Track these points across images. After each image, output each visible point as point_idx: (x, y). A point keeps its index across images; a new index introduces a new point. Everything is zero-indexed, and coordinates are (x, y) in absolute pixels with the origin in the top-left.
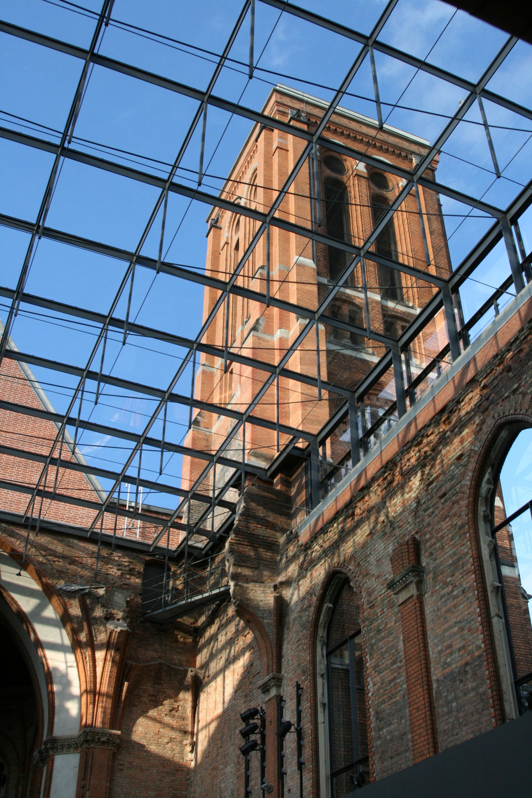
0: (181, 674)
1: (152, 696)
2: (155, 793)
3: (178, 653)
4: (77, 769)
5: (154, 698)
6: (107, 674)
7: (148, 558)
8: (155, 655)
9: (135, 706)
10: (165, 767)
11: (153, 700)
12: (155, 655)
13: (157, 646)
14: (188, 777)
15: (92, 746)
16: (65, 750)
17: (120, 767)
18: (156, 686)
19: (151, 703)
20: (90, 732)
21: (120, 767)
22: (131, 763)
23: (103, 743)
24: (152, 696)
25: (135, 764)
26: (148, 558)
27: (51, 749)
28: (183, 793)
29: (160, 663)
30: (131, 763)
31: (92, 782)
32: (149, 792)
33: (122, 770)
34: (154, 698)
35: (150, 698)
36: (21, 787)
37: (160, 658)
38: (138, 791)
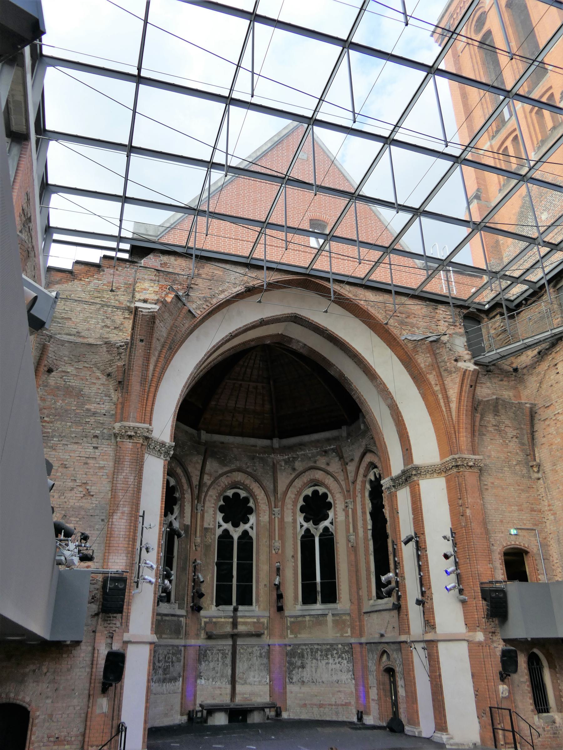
0: (515, 407)
1: (495, 426)
2: (517, 508)
3: (505, 389)
4: (445, 491)
5: (497, 428)
6: (463, 408)
7: (465, 311)
8: (489, 391)
9: (484, 435)
10: (519, 486)
11: (497, 430)
12: (489, 391)
13: (489, 384)
14: (538, 493)
15: (461, 470)
16: (428, 476)
17: (486, 487)
18: (496, 417)
19: (496, 432)
20: (459, 458)
21: (486, 487)
22: (493, 483)
23: (471, 467)
24: (495, 426)
25: (496, 484)
26: (465, 311)
27: (415, 475)
28: (538, 506)
29: (497, 399)
30: (493, 483)
31: (469, 501)
32: (513, 507)
33: (487, 489)
34: (497, 428)
35: (494, 428)
36: (350, 511)
37: (493, 394)
38: (503, 507)
